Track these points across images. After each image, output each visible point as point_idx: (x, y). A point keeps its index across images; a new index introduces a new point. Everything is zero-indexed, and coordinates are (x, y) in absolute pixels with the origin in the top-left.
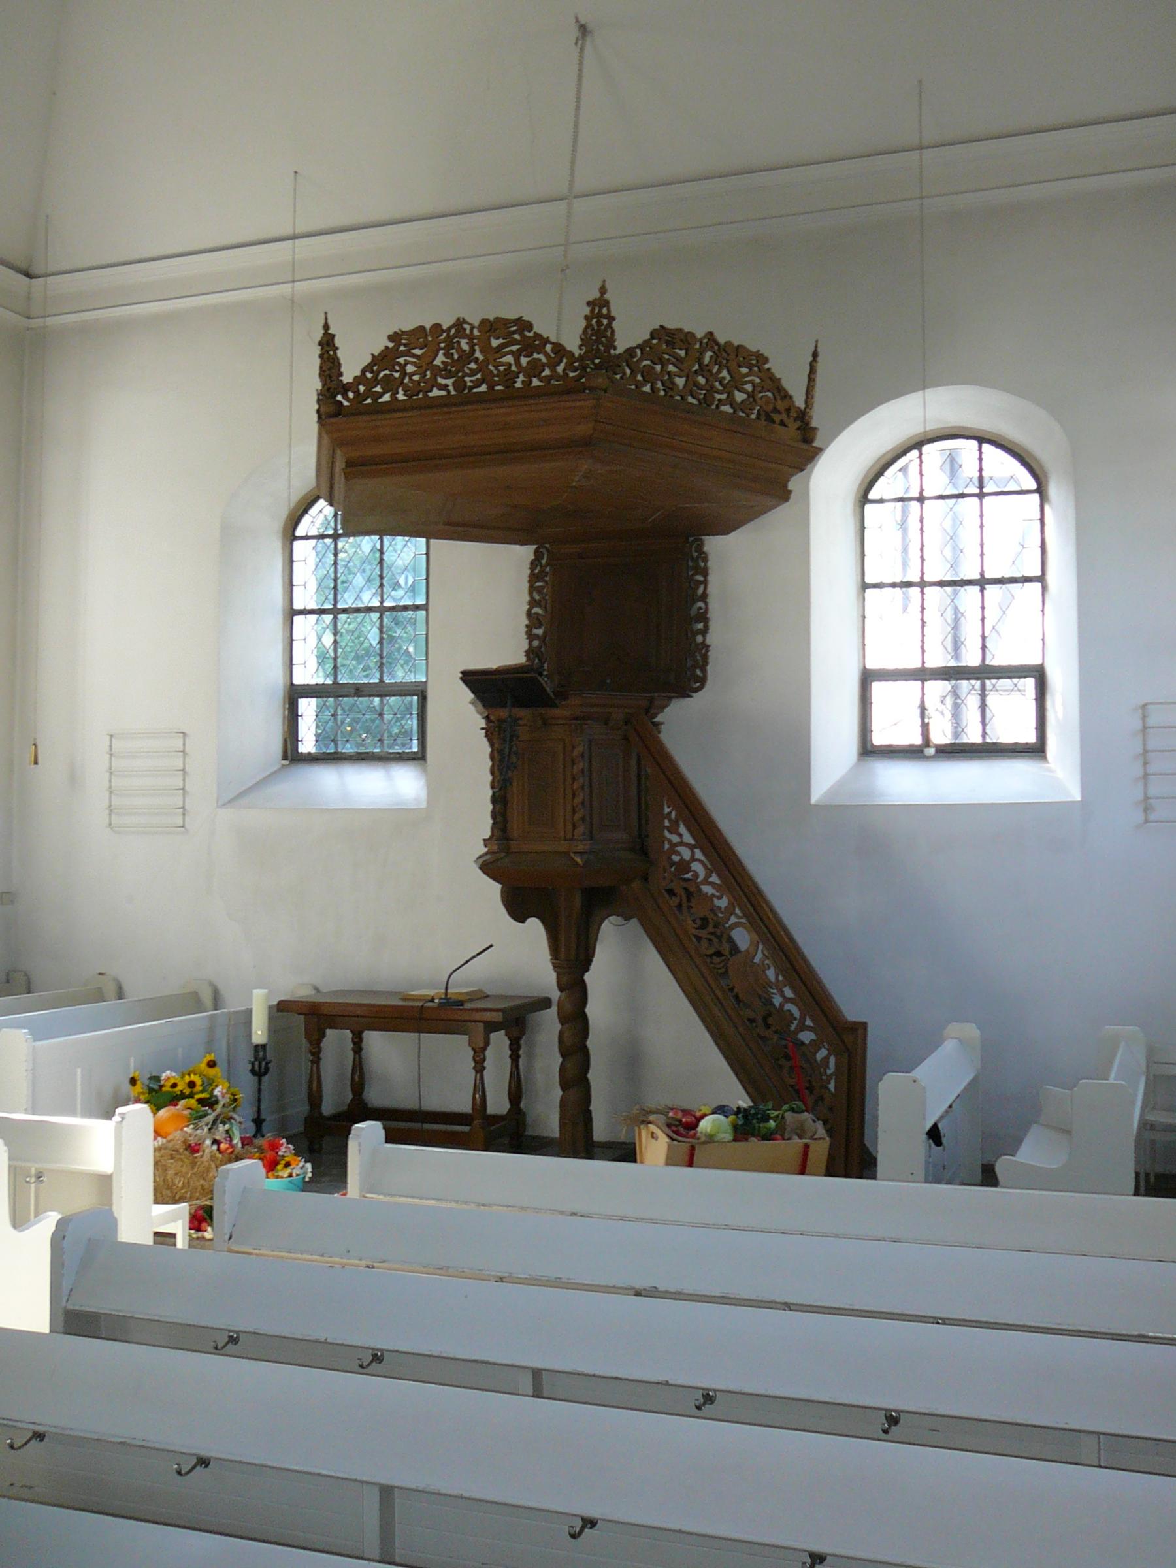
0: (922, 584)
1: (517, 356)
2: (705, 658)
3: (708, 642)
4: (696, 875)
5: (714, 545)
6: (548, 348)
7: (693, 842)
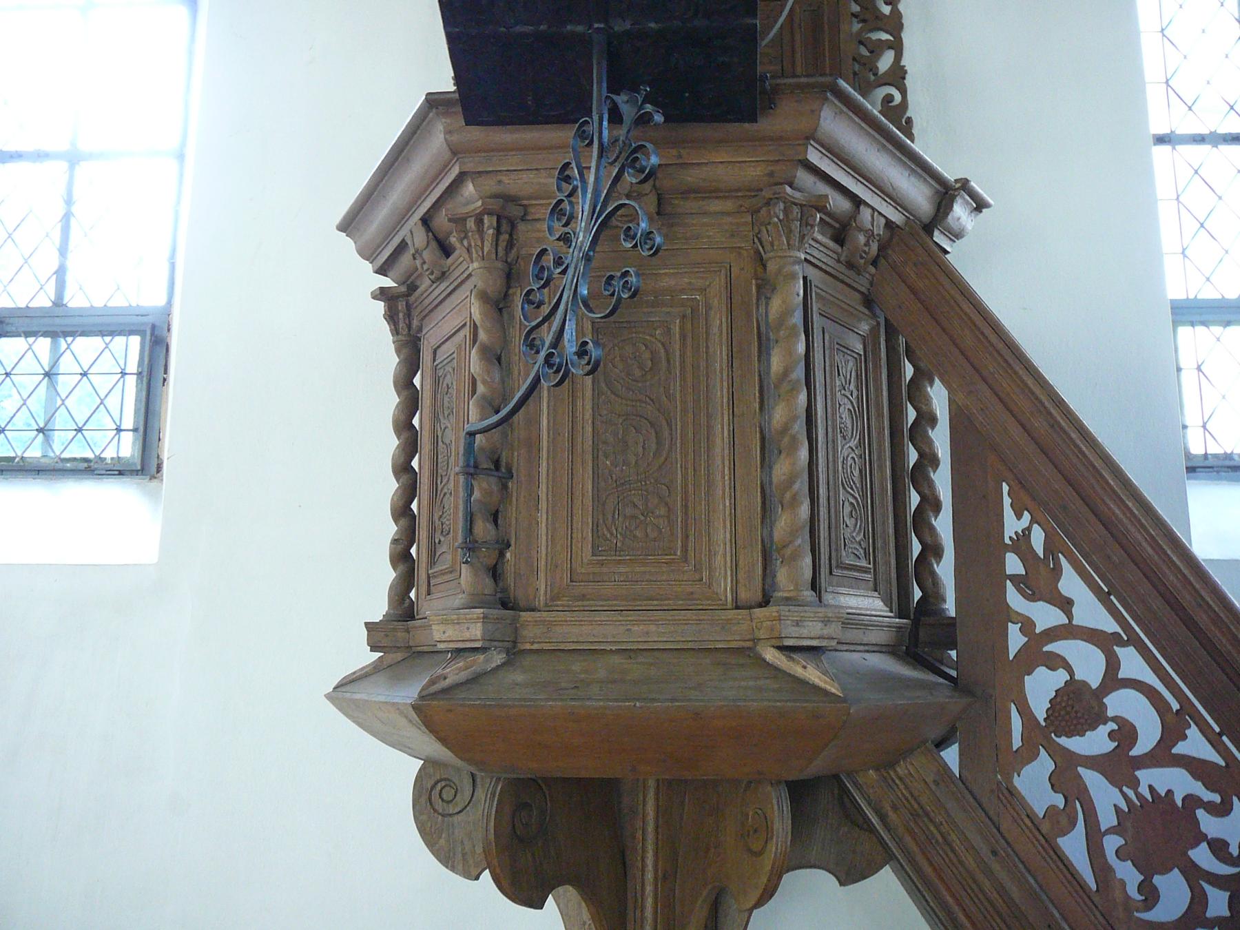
4: (1125, 733)
7: (1111, 626)
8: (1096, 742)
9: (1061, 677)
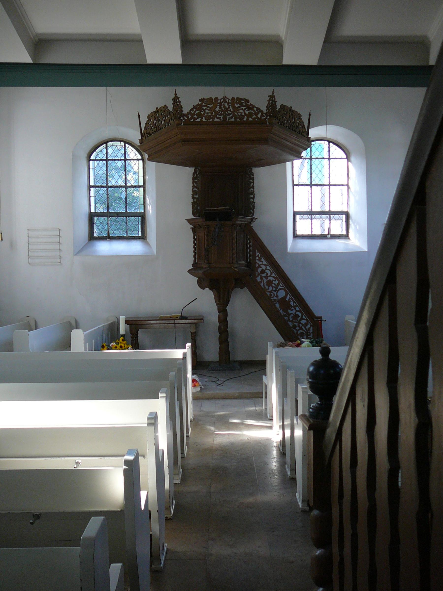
0: (330, 185)
1: (244, 110)
2: (254, 207)
3: (254, 201)
5: (256, 171)
6: (255, 109)
8: (264, 275)
9: (261, 269)
